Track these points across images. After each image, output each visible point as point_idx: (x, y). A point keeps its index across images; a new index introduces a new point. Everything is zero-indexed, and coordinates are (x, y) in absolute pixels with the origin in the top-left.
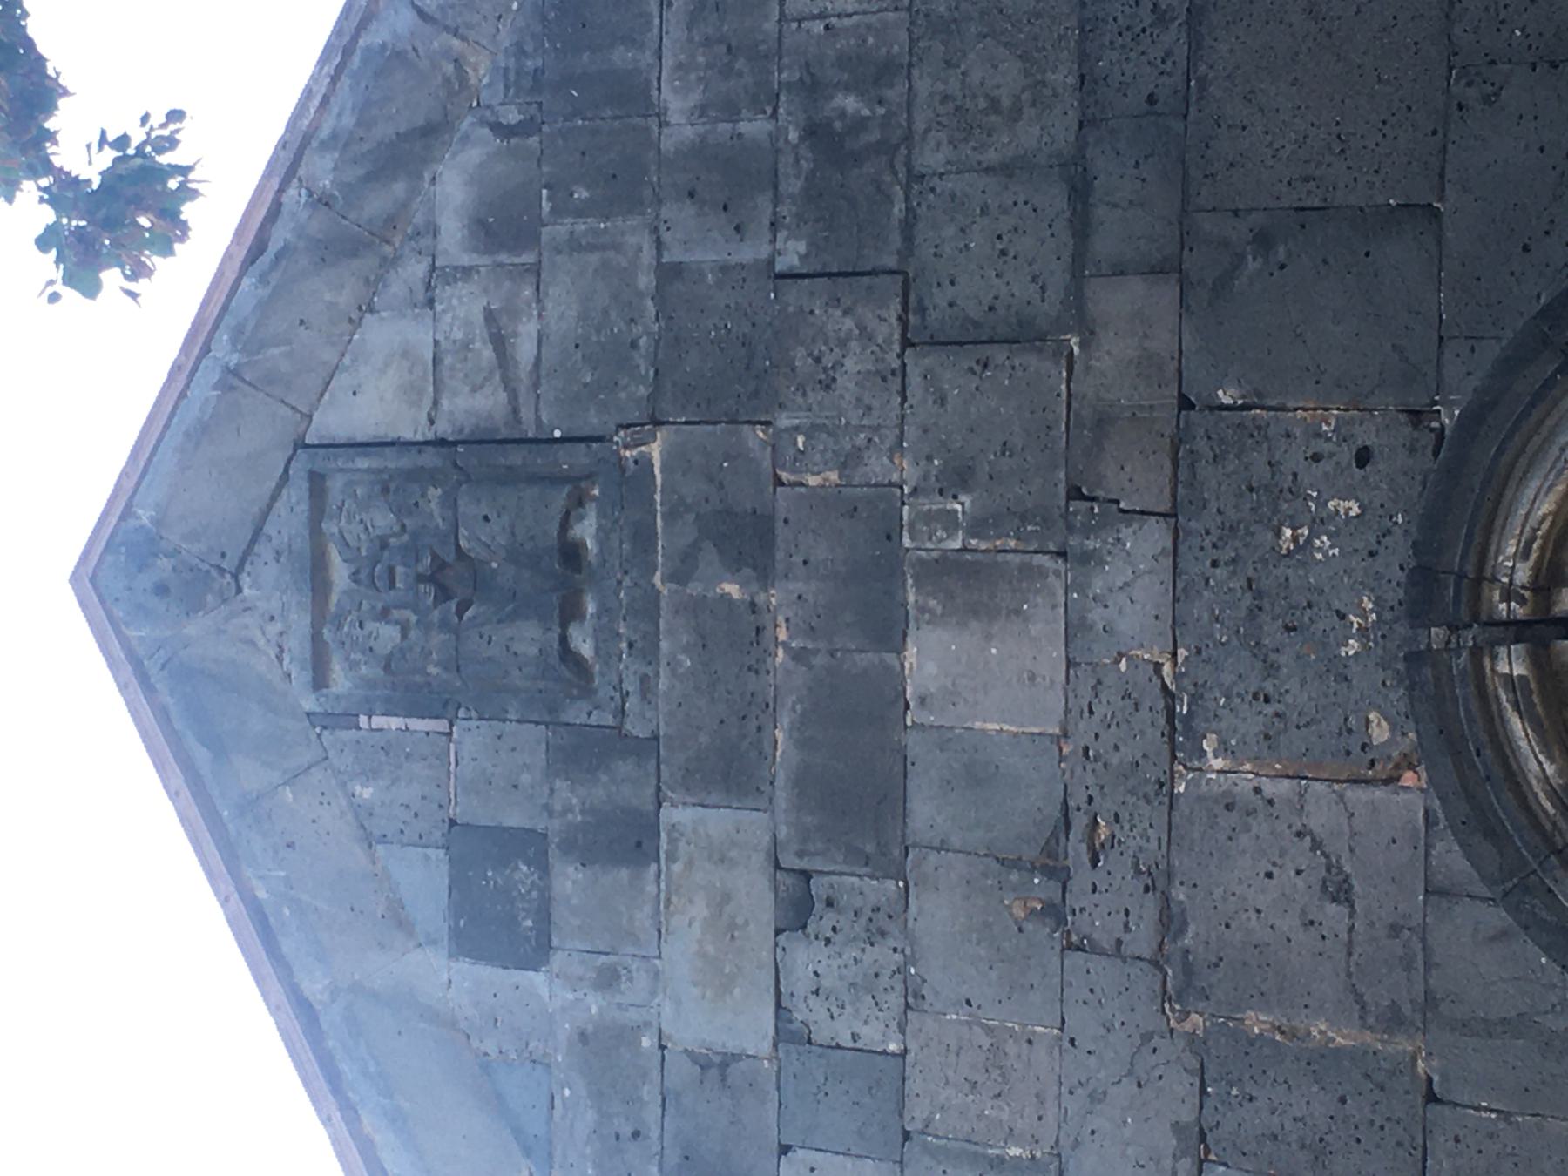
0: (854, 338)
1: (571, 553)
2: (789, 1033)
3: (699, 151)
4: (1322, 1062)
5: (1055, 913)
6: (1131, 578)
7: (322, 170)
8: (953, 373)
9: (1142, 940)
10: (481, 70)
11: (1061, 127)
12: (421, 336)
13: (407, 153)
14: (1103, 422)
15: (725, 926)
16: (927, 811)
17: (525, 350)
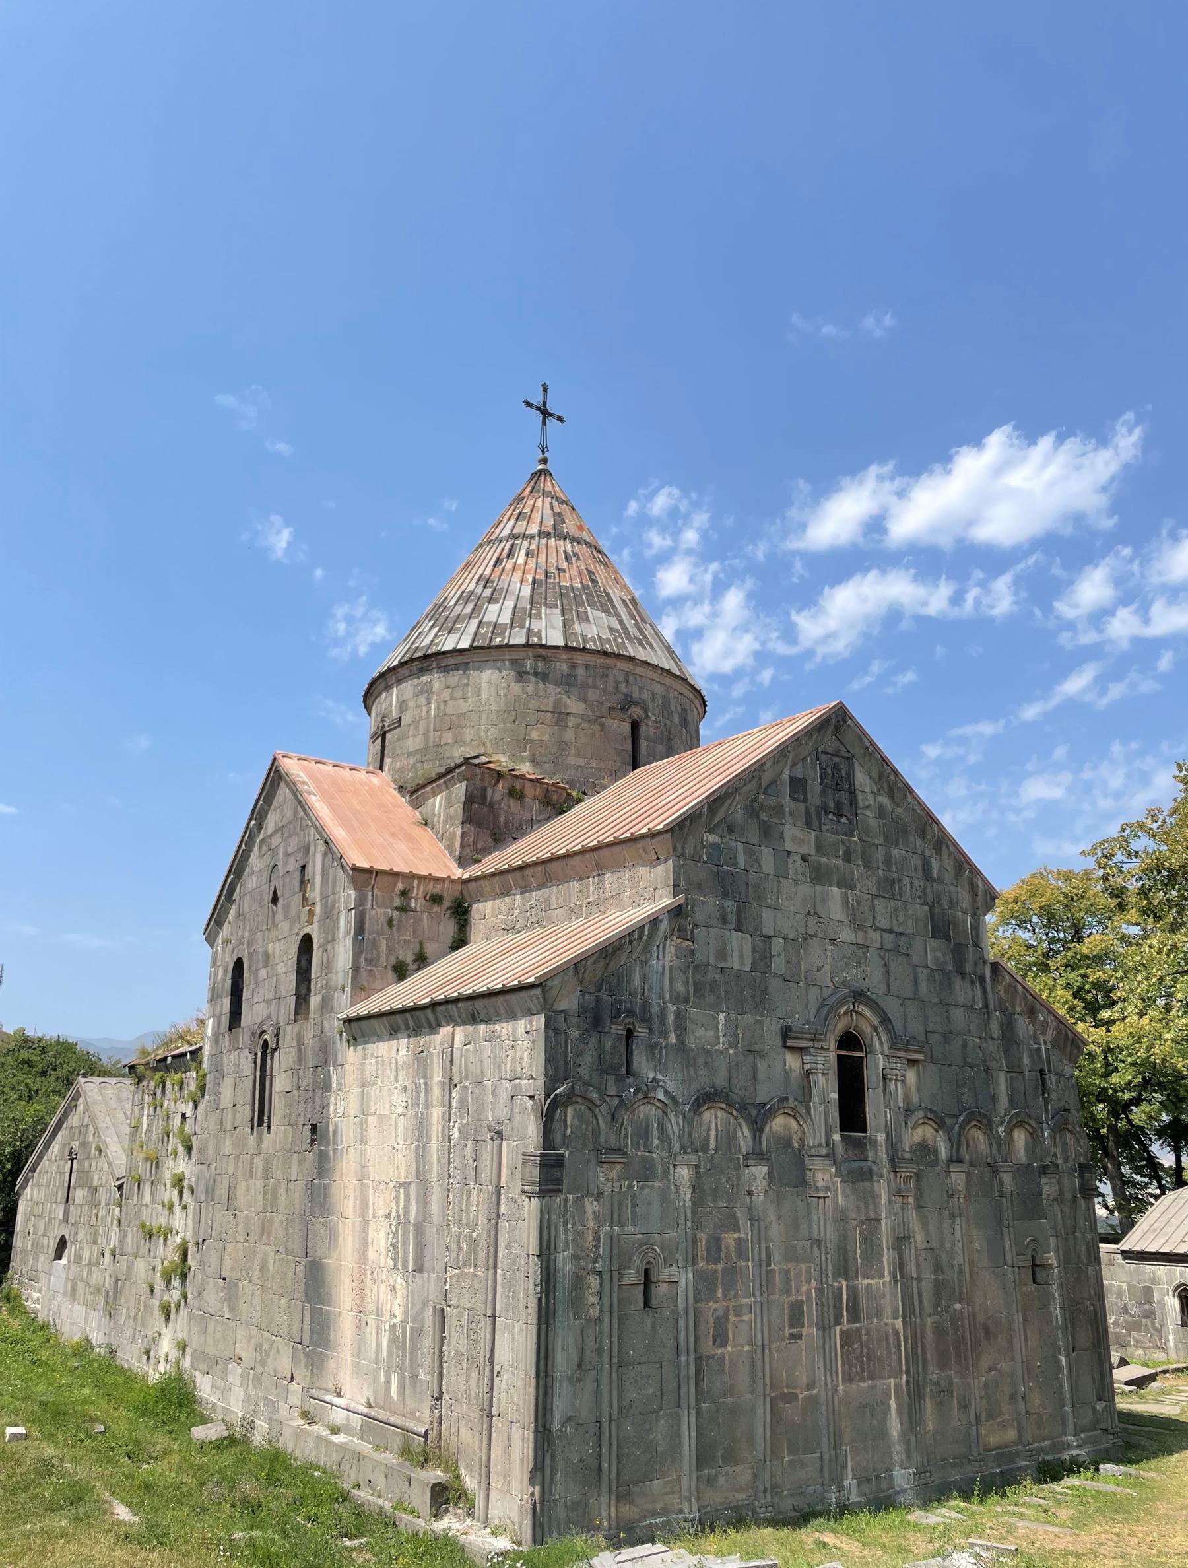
0: (871, 885)
1: (841, 816)
2: (789, 853)
3: (891, 856)
4: (799, 963)
5: (809, 913)
6: (846, 935)
7: (892, 777)
8: (869, 904)
9: (810, 932)
10: (899, 810)
11: (896, 929)
12: (867, 790)
13: (891, 795)
14: (865, 932)
15: (800, 842)
16: (819, 888)
17: (868, 813)
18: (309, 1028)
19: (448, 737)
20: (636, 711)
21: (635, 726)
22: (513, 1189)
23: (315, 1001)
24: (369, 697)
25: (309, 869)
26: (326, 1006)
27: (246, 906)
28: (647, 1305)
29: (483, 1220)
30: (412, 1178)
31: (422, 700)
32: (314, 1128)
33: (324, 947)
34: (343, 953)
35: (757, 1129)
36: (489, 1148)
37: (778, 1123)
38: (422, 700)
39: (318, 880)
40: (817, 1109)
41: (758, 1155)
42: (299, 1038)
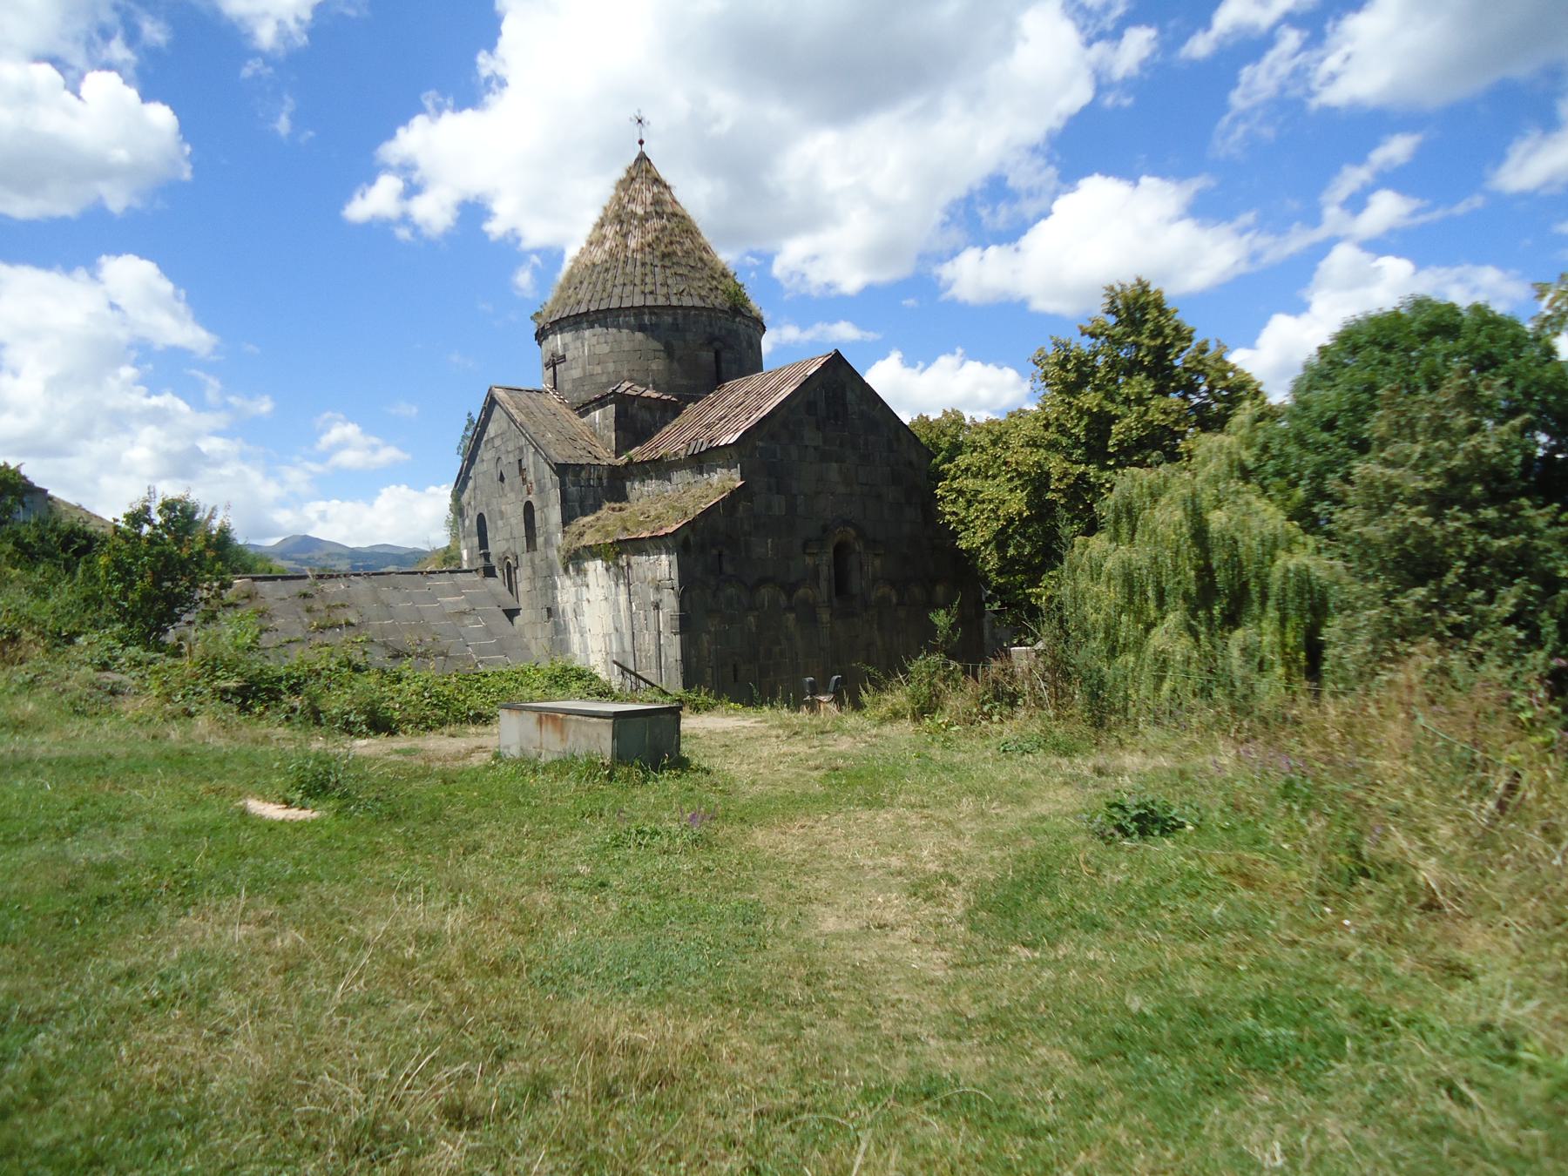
18: (537, 556)
19: (598, 369)
20: (717, 344)
21: (717, 353)
22: (665, 633)
23: (540, 540)
24: (541, 336)
25: (524, 462)
26: (547, 542)
27: (480, 480)
28: (736, 680)
29: (652, 647)
30: (612, 630)
31: (579, 344)
32: (549, 610)
33: (541, 509)
34: (555, 515)
35: (790, 596)
36: (653, 613)
37: (801, 592)
38: (579, 344)
39: (532, 469)
40: (823, 584)
41: (790, 609)
42: (532, 561)
